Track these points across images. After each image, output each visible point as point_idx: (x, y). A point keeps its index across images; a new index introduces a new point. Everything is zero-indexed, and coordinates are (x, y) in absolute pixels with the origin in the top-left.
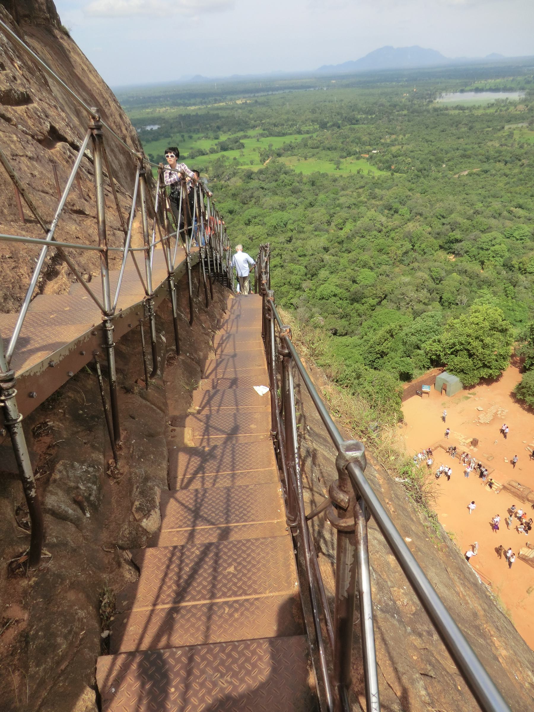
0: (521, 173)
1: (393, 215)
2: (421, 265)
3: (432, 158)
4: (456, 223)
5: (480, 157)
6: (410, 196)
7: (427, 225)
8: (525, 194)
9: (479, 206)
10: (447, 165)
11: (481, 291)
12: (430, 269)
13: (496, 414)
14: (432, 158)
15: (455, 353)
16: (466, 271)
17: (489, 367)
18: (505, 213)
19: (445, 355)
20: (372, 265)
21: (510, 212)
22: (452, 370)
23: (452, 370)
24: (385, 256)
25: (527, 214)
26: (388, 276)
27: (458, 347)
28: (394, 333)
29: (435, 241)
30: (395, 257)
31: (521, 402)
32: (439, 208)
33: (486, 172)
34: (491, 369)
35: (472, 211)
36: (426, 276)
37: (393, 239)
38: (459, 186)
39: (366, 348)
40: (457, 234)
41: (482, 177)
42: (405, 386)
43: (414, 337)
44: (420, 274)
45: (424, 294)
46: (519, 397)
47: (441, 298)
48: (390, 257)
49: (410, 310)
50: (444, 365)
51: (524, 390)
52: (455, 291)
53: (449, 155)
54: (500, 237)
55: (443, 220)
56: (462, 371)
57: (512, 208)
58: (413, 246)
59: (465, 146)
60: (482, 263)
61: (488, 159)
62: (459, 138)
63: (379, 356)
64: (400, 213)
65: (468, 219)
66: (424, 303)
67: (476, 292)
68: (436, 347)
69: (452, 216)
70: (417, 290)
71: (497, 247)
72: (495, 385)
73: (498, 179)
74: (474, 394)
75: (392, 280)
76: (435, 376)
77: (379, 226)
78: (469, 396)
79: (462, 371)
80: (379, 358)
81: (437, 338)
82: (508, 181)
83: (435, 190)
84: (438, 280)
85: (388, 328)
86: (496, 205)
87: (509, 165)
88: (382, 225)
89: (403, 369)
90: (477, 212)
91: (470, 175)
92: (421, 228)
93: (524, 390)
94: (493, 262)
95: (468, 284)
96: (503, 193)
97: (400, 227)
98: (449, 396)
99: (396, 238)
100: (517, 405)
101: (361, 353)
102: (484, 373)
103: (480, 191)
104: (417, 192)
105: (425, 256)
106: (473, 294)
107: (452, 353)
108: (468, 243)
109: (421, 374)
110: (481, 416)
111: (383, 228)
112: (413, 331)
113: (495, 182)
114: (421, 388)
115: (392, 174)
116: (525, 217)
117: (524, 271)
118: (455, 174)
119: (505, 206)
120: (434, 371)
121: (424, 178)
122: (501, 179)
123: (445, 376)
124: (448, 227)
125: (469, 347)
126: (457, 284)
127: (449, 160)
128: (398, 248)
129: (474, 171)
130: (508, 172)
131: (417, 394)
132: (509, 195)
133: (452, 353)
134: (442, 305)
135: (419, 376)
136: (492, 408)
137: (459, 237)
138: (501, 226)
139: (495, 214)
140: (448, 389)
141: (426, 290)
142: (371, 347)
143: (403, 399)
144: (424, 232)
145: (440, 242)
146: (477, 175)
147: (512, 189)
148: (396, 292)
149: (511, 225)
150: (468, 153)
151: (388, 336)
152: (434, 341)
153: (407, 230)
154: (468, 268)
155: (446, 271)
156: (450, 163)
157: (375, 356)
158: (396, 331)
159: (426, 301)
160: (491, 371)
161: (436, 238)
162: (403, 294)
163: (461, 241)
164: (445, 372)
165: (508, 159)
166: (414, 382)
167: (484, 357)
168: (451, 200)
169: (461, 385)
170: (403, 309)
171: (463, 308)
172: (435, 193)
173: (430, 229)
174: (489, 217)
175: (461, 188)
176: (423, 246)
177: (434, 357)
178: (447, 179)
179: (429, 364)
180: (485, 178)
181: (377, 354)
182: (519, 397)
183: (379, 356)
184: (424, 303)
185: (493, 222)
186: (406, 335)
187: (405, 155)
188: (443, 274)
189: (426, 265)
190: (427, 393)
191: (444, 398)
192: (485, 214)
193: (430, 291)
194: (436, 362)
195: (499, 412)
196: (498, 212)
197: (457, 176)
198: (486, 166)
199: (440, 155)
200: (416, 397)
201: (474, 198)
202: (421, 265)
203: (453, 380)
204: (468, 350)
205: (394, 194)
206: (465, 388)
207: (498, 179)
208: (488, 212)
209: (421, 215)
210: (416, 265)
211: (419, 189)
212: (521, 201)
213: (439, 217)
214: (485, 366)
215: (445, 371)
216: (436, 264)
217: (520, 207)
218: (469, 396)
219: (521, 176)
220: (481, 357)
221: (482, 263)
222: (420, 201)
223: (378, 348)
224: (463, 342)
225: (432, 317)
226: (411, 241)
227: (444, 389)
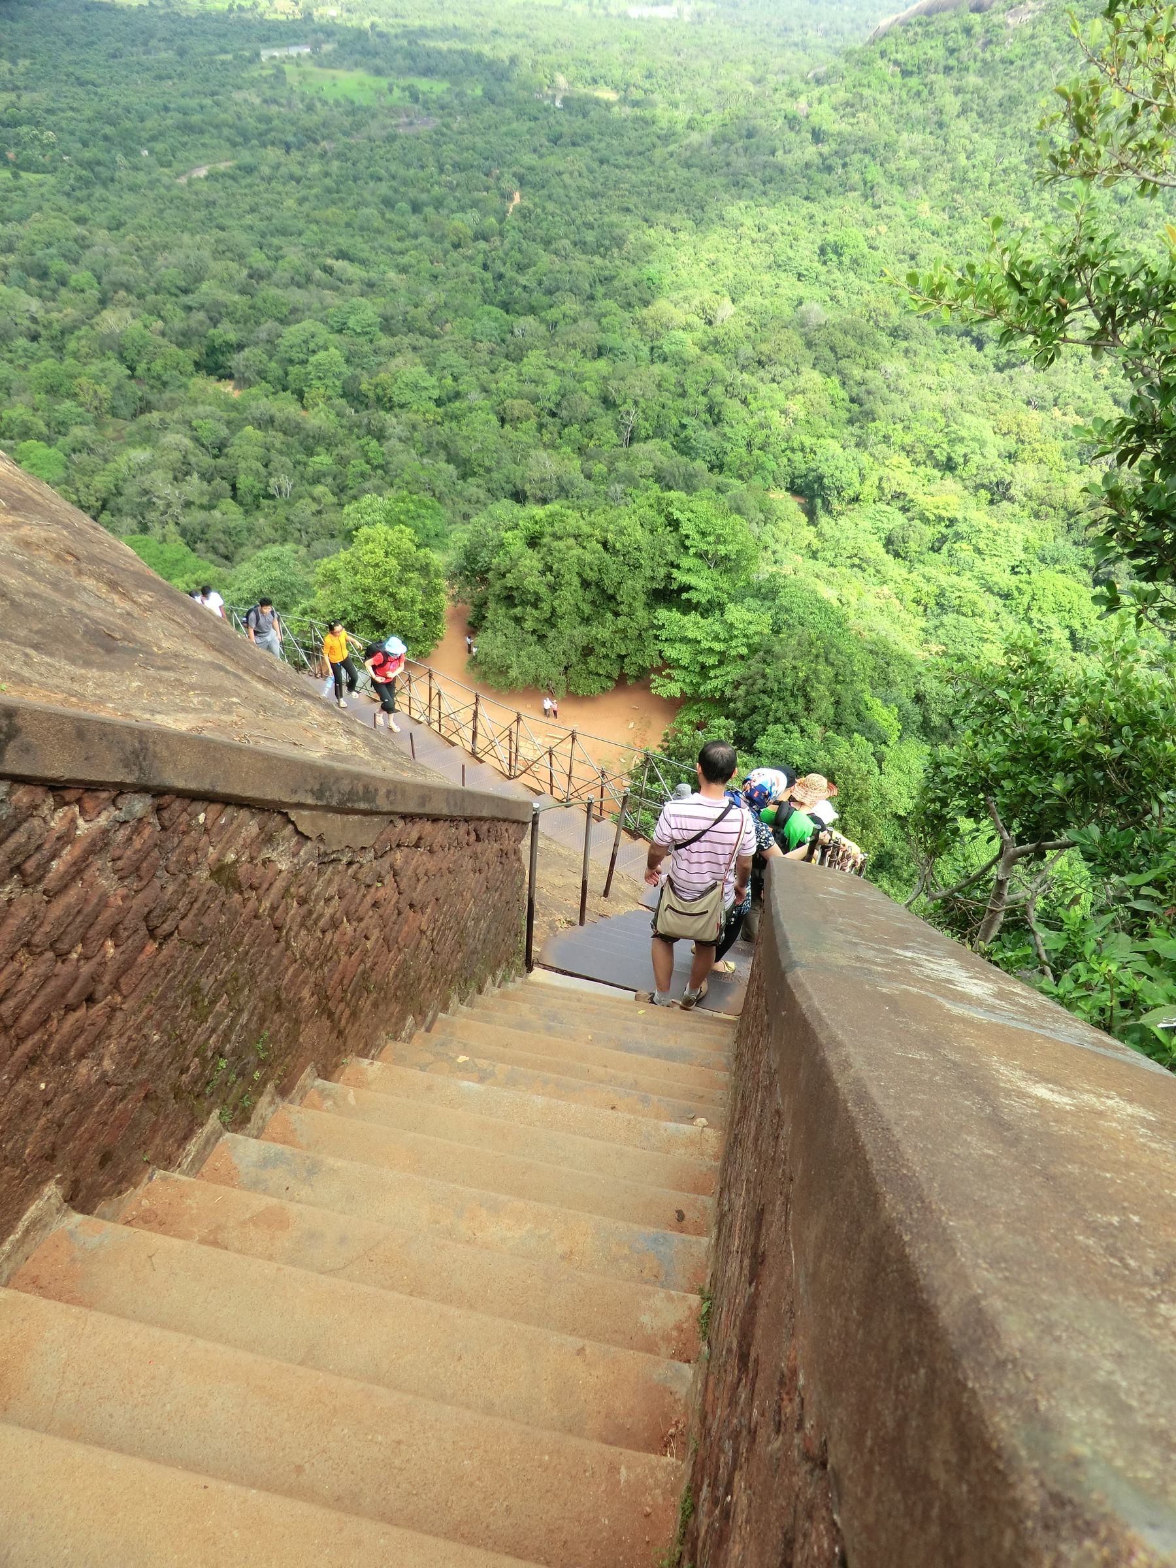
0: (327, 174)
1: (54, 291)
2: (168, 416)
3: (108, 130)
4: (217, 304)
5: (226, 131)
6: (84, 238)
7: (151, 313)
8: (348, 225)
9: (258, 259)
10: (151, 152)
11: (316, 459)
12: (189, 423)
14: (108, 130)
16: (272, 420)
18: (318, 274)
20: (45, 430)
21: (328, 270)
24: (68, 404)
25: (364, 274)
26: (91, 451)
29: (181, 352)
30: (96, 403)
32: (168, 268)
33: (249, 170)
35: (245, 272)
36: (188, 442)
37: (75, 355)
38: (196, 209)
40: (227, 332)
41: (244, 182)
45: (194, 485)
47: (234, 488)
48: (81, 405)
49: (172, 527)
52: (262, 470)
53: (149, 124)
55: (186, 300)
57: (329, 261)
58: (132, 369)
59: (184, 102)
60: (300, 395)
62: (160, 78)
64: (72, 283)
65: (242, 292)
66: (202, 507)
67: (305, 464)
69: (205, 286)
70: (175, 479)
71: (321, 355)
73: (280, 188)
75: (106, 461)
77: (27, 323)
82: (303, 192)
83: (142, 219)
84: (220, 449)
86: (294, 256)
87: (296, 155)
88: (34, 320)
90: (256, 275)
91: (212, 177)
92: (138, 324)
94: (322, 391)
95: (285, 449)
96: (301, 224)
97: (83, 323)
99: (84, 351)
103: (249, 219)
104: (100, 226)
105: (167, 395)
106: (300, 468)
108: (257, 351)
111: (40, 329)
113: (277, 197)
115: (16, 176)
116: (362, 281)
117: (386, 403)
118: (178, 176)
119: (314, 256)
121: (105, 185)
122: (287, 188)
124: (201, 315)
126: (260, 451)
127: (153, 138)
128: (97, 380)
129: (222, 167)
130: (297, 171)
132: (314, 227)
134: (241, 504)
137: (232, 337)
138: (317, 305)
139: (297, 278)
141: (195, 475)
144: (147, 333)
145: (194, 353)
146: (233, 178)
147: (317, 214)
148: (130, 490)
149: (338, 302)
150: (196, 118)
153: (104, 329)
154: (274, 411)
155: (229, 423)
156: (159, 147)
159: (205, 500)
161: (180, 345)
162: (146, 492)
163: (240, 347)
165: (290, 138)
170: (157, 530)
171: (288, 503)
172: (143, 228)
173: (160, 324)
174: (286, 286)
175: (201, 214)
176: (157, 366)
178: (162, 190)
180: (250, 186)
185: (298, 296)
188: (224, 432)
189: (176, 415)
192: (275, 277)
193: (207, 477)
196: (303, 270)
197: (183, 181)
198: (246, 157)
199: (128, 124)
201: (242, 238)
202: (168, 416)
205: (40, 232)
207: (280, 188)
209: (128, 289)
210: (154, 417)
211: (101, 218)
212: (344, 242)
213: (174, 290)
216: (200, 409)
217: (342, 255)
219: (328, 182)
221: (300, 395)
222: (113, 250)
226: (122, 358)
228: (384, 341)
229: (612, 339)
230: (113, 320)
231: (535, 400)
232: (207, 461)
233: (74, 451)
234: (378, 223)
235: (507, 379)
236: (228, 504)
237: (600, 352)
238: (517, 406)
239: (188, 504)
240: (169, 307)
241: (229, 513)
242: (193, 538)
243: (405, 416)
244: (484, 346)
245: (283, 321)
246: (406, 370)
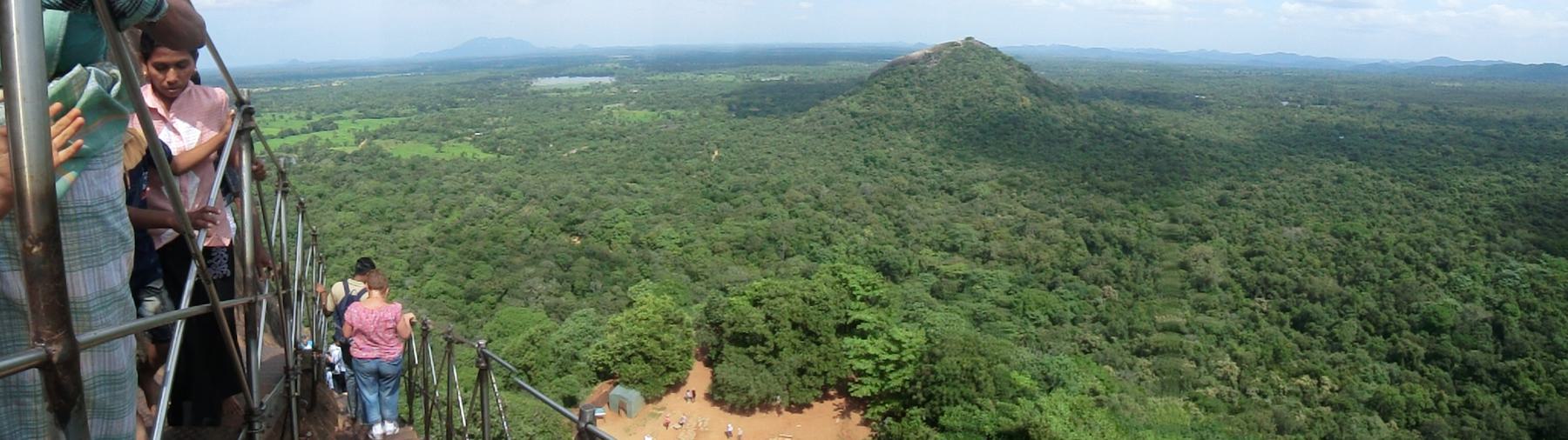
9: (594, 184)
15: (628, 359)
17: (675, 370)
27: (629, 352)
40: (577, 215)
44: (544, 262)
50: (613, 377)
54: (622, 214)
61: (594, 136)
68: (601, 355)
74: (663, 409)
84: (567, 267)
85: (527, 334)
86: (611, 181)
90: (594, 190)
102: (670, 379)
117: (654, 247)
120: (603, 386)
123: (619, 390)
168: (565, 180)
169: (642, 400)
170: (533, 306)
185: (612, 198)
187: (510, 136)
193: (560, 281)
194: (604, 374)
198: (593, 144)
201: (589, 176)
203: (633, 395)
208: (605, 188)
214: (669, 370)
217: (635, 182)
221: (609, 242)
228: (653, 218)
229: (769, 210)
230: (526, 210)
231: (729, 242)
232: (561, 273)
234: (651, 166)
235: (716, 231)
236: (569, 294)
237: (764, 216)
238: (720, 245)
240: (552, 204)
241: (568, 299)
242: (550, 310)
243: (662, 252)
244: (703, 217)
245: (604, 209)
246: (664, 231)
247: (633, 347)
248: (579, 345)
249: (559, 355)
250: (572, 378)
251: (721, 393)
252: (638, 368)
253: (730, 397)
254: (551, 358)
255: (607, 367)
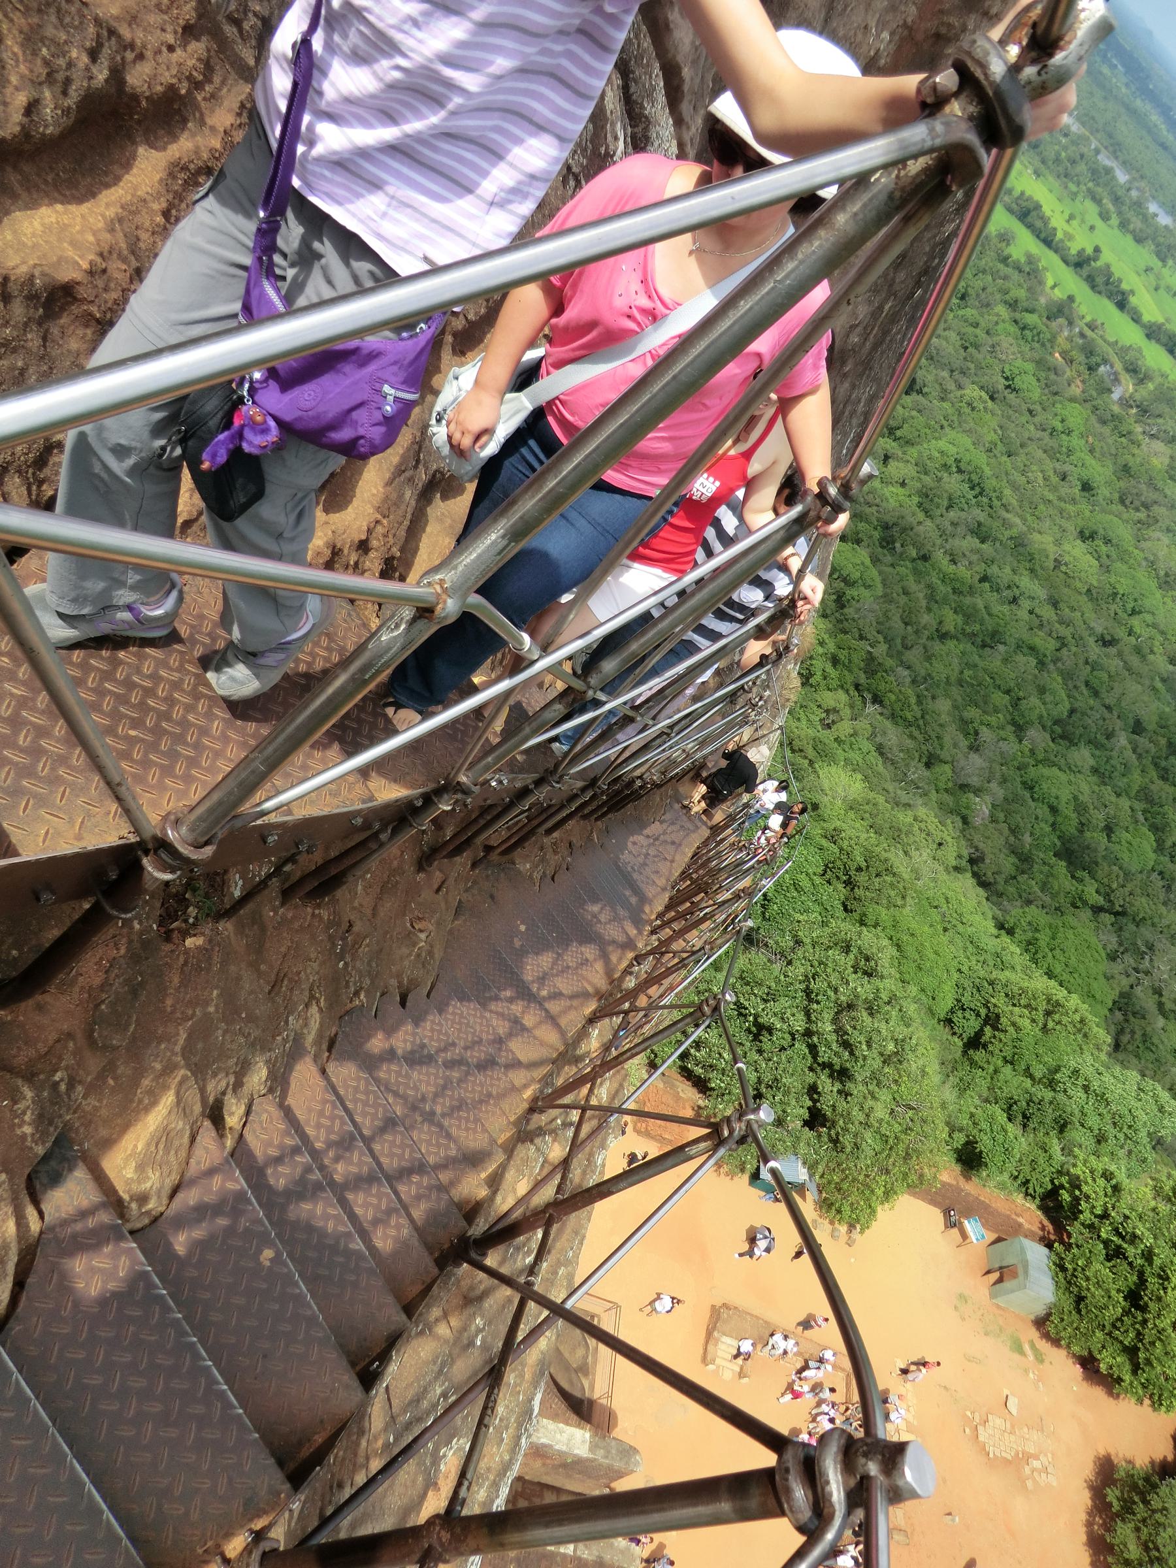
13: (1027, 1457)
15: (1114, 1254)
17: (1136, 1369)
19: (1091, 1227)
22: (1063, 1269)
23: (1063, 1269)
27: (1131, 1251)
28: (1057, 1017)
31: (1100, 1505)
34: (1135, 1372)
39: (982, 973)
42: (948, 1173)
43: (1081, 1094)
46: (1112, 1495)
51: (1140, 1508)
56: (1080, 1299)
63: (983, 1012)
66: (1160, 1005)
68: (1095, 1189)
72: (1098, 1393)
74: (1040, 1358)
75: (1165, 904)
76: (1020, 1225)
78: (1027, 1348)
79: (1080, 1299)
80: (978, 1015)
81: (1121, 1176)
85: (1060, 994)
89: (985, 1143)
93: (1140, 1508)
98: (993, 1296)
100: (1084, 1499)
101: (965, 969)
102: (1110, 1359)
107: (1106, 1243)
109: (1002, 1186)
110: (996, 1421)
112: (1095, 1085)
114: (968, 1213)
120: (1030, 1215)
123: (1037, 1255)
125: (1152, 1282)
131: (947, 1212)
133: (1106, 1243)
135: (992, 1189)
136: (1035, 1435)
140: (1007, 1285)
142: (991, 983)
143: (912, 1189)
148: (1146, 932)
151: (1043, 1006)
152: (1107, 1176)
157: (977, 1004)
158: (1065, 1020)
160: (1127, 1377)
162: (1151, 947)
164: (1046, 1250)
166: (971, 1188)
167: (1153, 1344)
169: (1040, 1310)
170: (1117, 968)
177: (1065, 1196)
179: (1040, 1190)
181: (986, 1006)
182: (1112, 1495)
183: (983, 1012)
184: (1160, 1005)
186: (1076, 1072)
190: (964, 1236)
191: (980, 1288)
194: (1059, 1208)
195: (1036, 1464)
200: (935, 1216)
203: (1040, 1288)
204: (1142, 1280)
206: (1040, 1323)
214: (1131, 1352)
215: (1049, 1246)
218: (1027, 1348)
220: (1149, 1334)
223: (999, 1001)
224: (1157, 1262)
225: (1161, 1109)
227: (1002, 1274)
233: (1161, 873)
239: (1158, 992)
247: (1148, 1255)
248: (1093, 1121)
249: (1052, 1084)
250: (1021, 1142)
251: (1128, 1508)
252: (1107, 1283)
253: (1125, 1532)
254: (1038, 1071)
255: (1075, 1212)
